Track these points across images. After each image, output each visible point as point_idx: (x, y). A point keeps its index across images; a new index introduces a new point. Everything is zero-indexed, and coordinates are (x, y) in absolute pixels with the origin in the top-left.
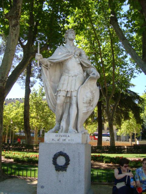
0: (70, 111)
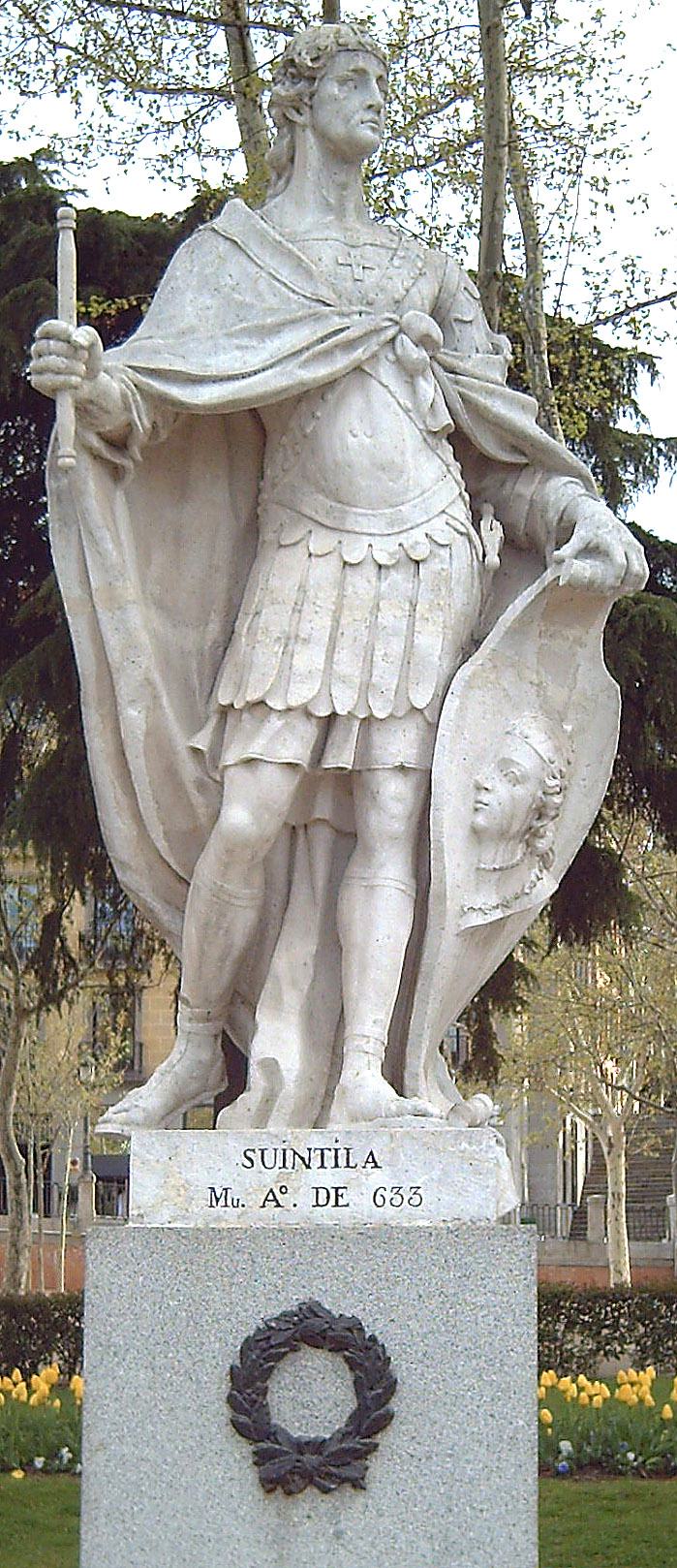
0: (344, 906)
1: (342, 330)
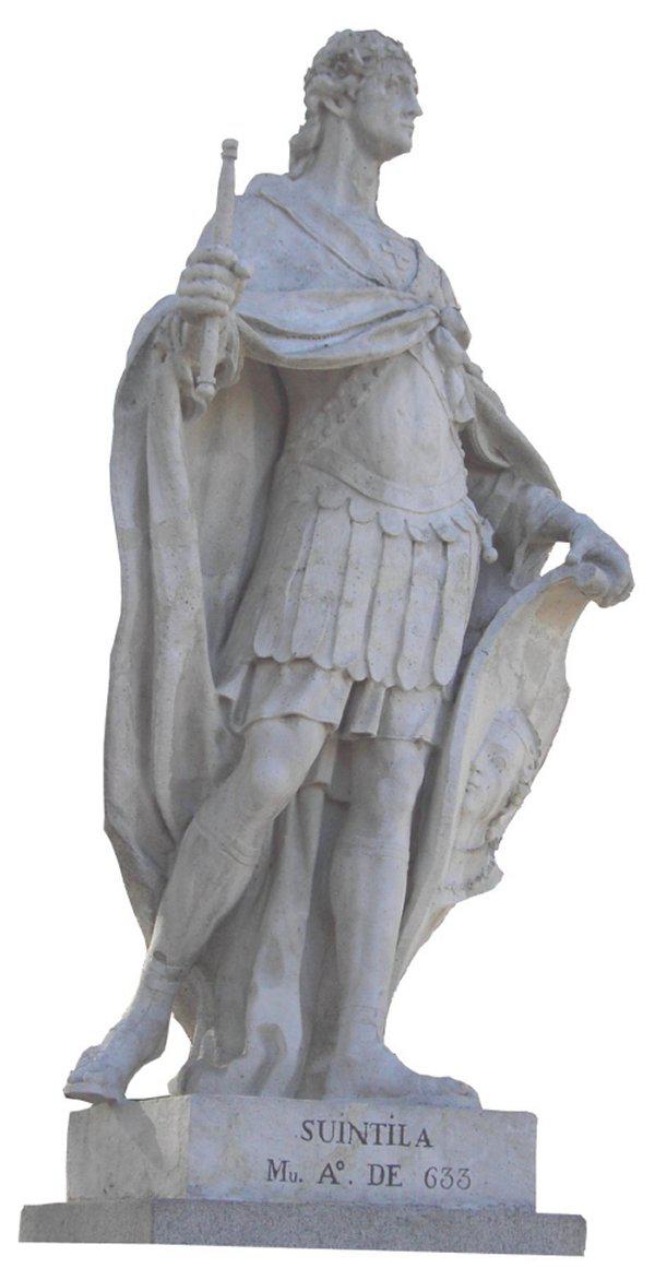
1: (399, 313)
